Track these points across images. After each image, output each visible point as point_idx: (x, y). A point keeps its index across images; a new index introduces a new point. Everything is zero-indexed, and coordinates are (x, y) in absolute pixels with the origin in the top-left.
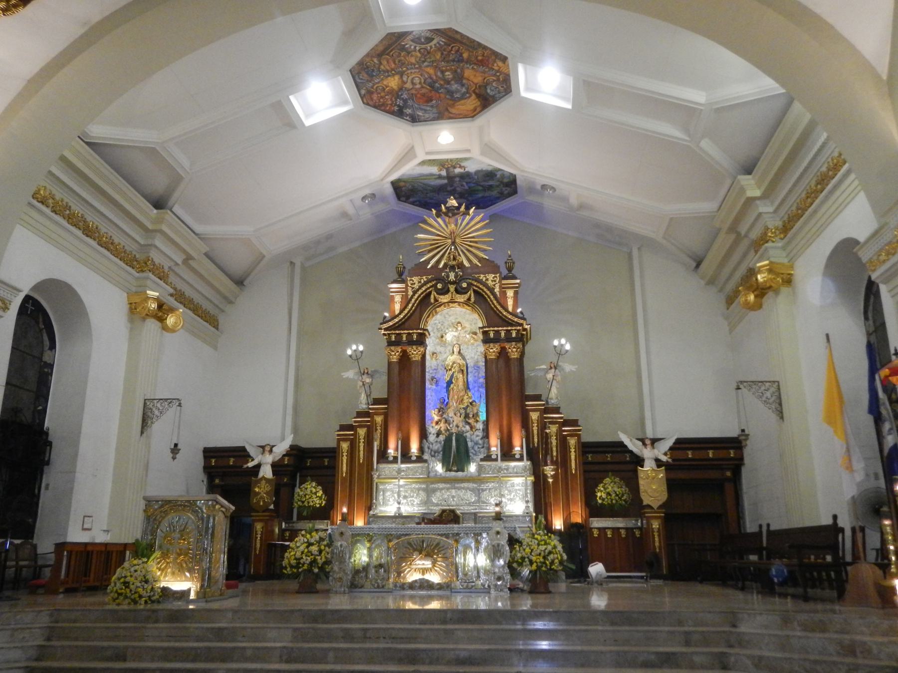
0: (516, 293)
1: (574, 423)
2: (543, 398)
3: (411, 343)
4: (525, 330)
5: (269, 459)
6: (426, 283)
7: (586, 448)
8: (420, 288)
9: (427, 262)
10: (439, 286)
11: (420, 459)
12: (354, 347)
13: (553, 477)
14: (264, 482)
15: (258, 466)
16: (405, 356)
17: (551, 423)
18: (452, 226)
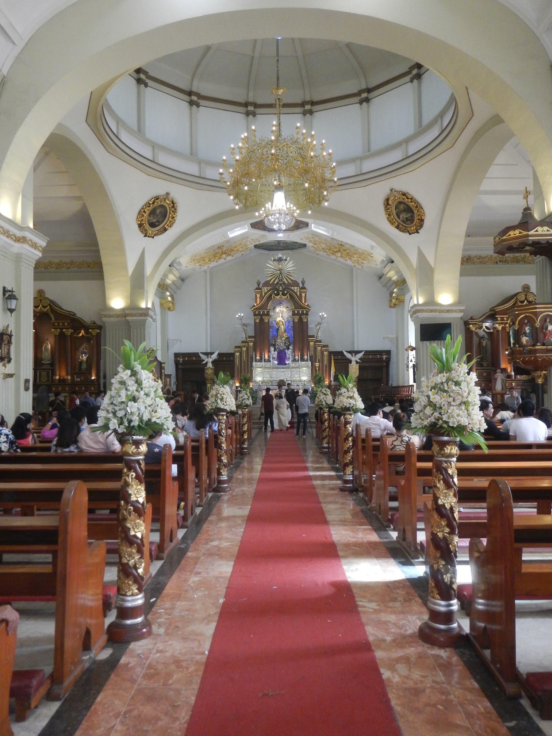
0: (306, 295)
1: (327, 346)
2: (315, 336)
3: (264, 314)
4: (309, 309)
5: (210, 360)
6: (270, 290)
7: (330, 353)
8: (268, 292)
9: (270, 280)
10: (276, 292)
11: (269, 361)
12: (239, 314)
13: (319, 367)
14: (209, 369)
15: (206, 363)
16: (262, 320)
17: (318, 346)
18: (280, 266)
